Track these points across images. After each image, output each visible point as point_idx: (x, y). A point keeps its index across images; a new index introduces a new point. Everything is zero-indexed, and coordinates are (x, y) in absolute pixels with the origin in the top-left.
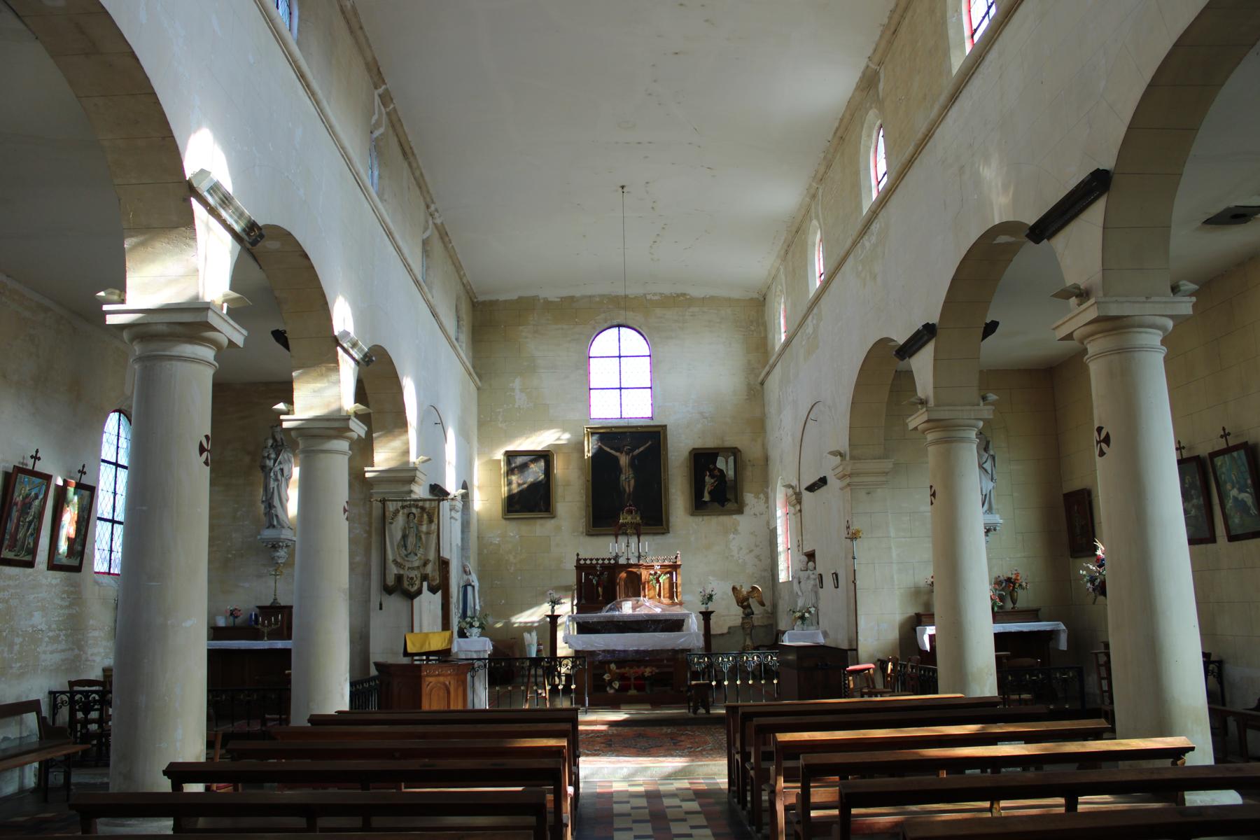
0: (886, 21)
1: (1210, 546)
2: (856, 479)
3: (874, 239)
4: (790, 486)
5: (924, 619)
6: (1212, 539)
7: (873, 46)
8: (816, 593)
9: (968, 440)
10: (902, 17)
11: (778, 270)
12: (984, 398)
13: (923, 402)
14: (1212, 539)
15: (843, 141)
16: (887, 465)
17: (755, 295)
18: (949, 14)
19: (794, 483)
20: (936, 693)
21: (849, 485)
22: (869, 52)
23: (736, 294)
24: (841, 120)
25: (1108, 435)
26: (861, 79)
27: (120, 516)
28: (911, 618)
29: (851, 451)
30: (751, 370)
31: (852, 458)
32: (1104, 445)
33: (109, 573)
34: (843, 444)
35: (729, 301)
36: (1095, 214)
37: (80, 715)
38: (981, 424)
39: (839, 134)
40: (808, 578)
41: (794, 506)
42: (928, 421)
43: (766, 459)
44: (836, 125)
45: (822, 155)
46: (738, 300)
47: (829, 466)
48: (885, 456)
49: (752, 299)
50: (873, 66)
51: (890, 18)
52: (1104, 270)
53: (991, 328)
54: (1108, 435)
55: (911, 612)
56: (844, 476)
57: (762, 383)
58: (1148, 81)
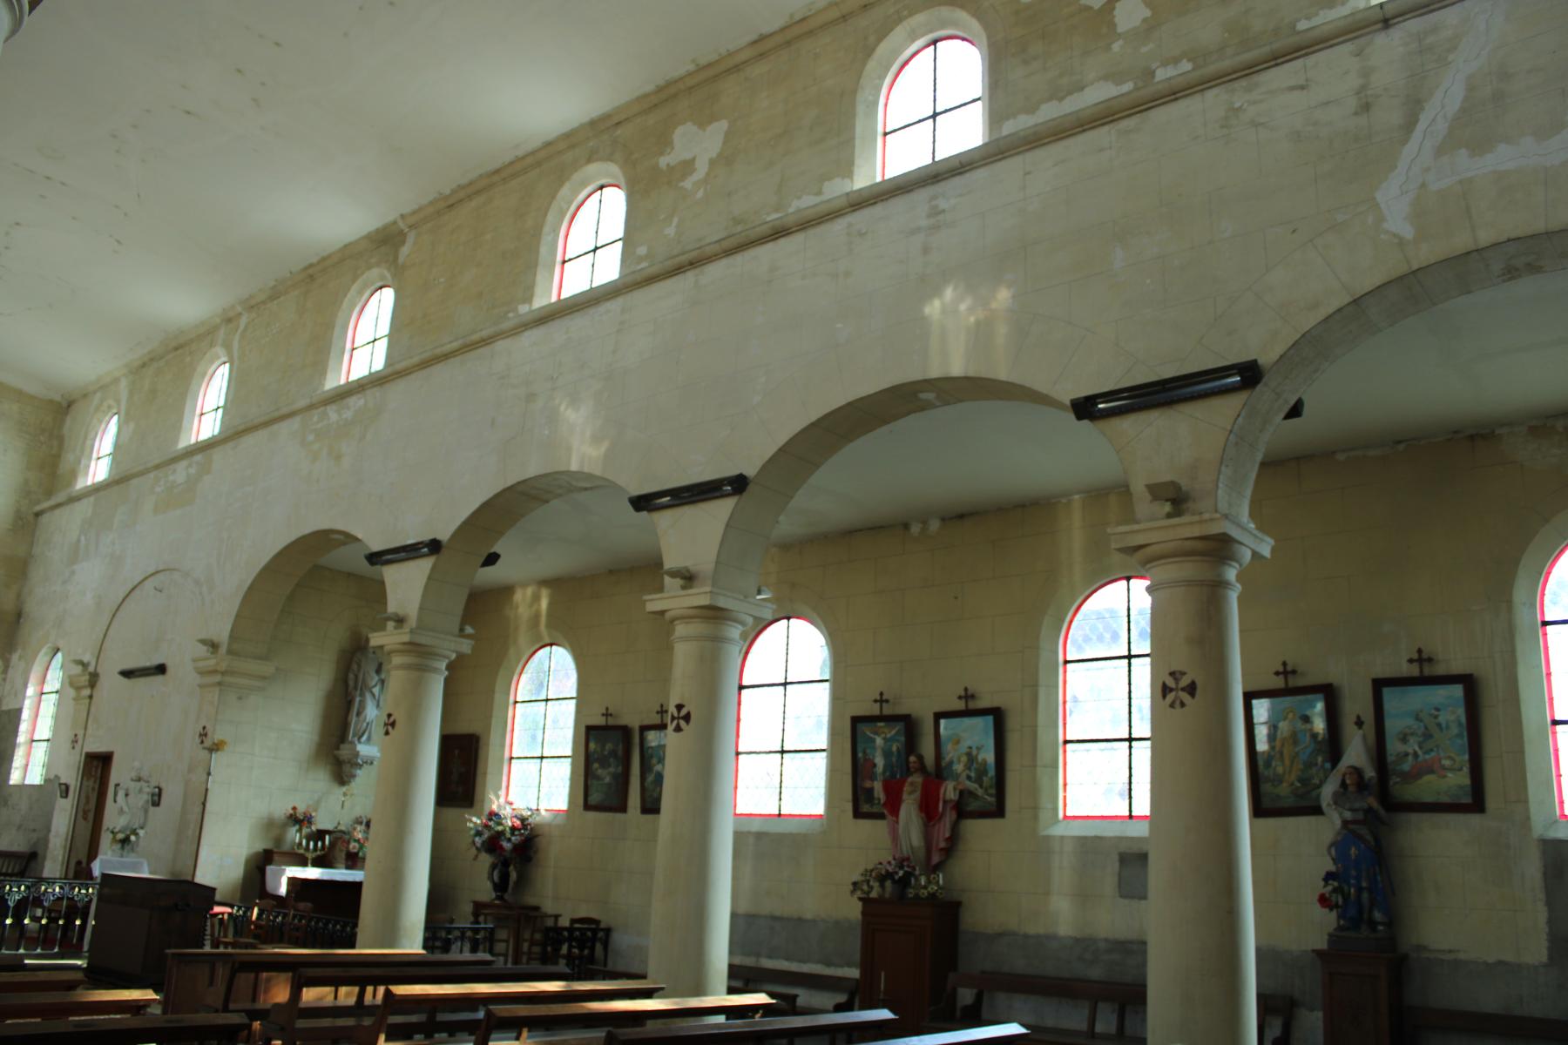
0: (448, 192)
1: (619, 816)
2: (229, 679)
3: (348, 414)
4: (84, 665)
5: (276, 857)
6: (622, 808)
7: (415, 207)
8: (146, 811)
9: (435, 670)
10: (470, 197)
11: (116, 381)
12: (462, 630)
13: (400, 621)
14: (622, 808)
15: (323, 284)
16: (268, 668)
17: (57, 398)
18: (546, 229)
19: (87, 657)
20: (353, 947)
21: (219, 684)
22: (406, 210)
23: (32, 389)
24: (324, 259)
25: (688, 714)
26: (377, 231)
27: (1143, 728)
28: (257, 854)
29: (229, 644)
30: (25, 492)
31: (230, 652)
32: (682, 723)
33: (738, 754)
34: (221, 630)
35: (19, 395)
36: (721, 510)
37: (576, 951)
38: (454, 656)
39: (310, 271)
40: (140, 791)
41: (78, 689)
42: (410, 643)
43: (19, 615)
44: (314, 260)
45: (272, 283)
46: (32, 397)
47: (183, 655)
48: (265, 658)
49: (51, 401)
50: (401, 224)
51: (454, 192)
52: (717, 562)
53: (492, 559)
54: (688, 714)
55: (260, 846)
56: (213, 672)
57: (38, 515)
58: (814, 418)
